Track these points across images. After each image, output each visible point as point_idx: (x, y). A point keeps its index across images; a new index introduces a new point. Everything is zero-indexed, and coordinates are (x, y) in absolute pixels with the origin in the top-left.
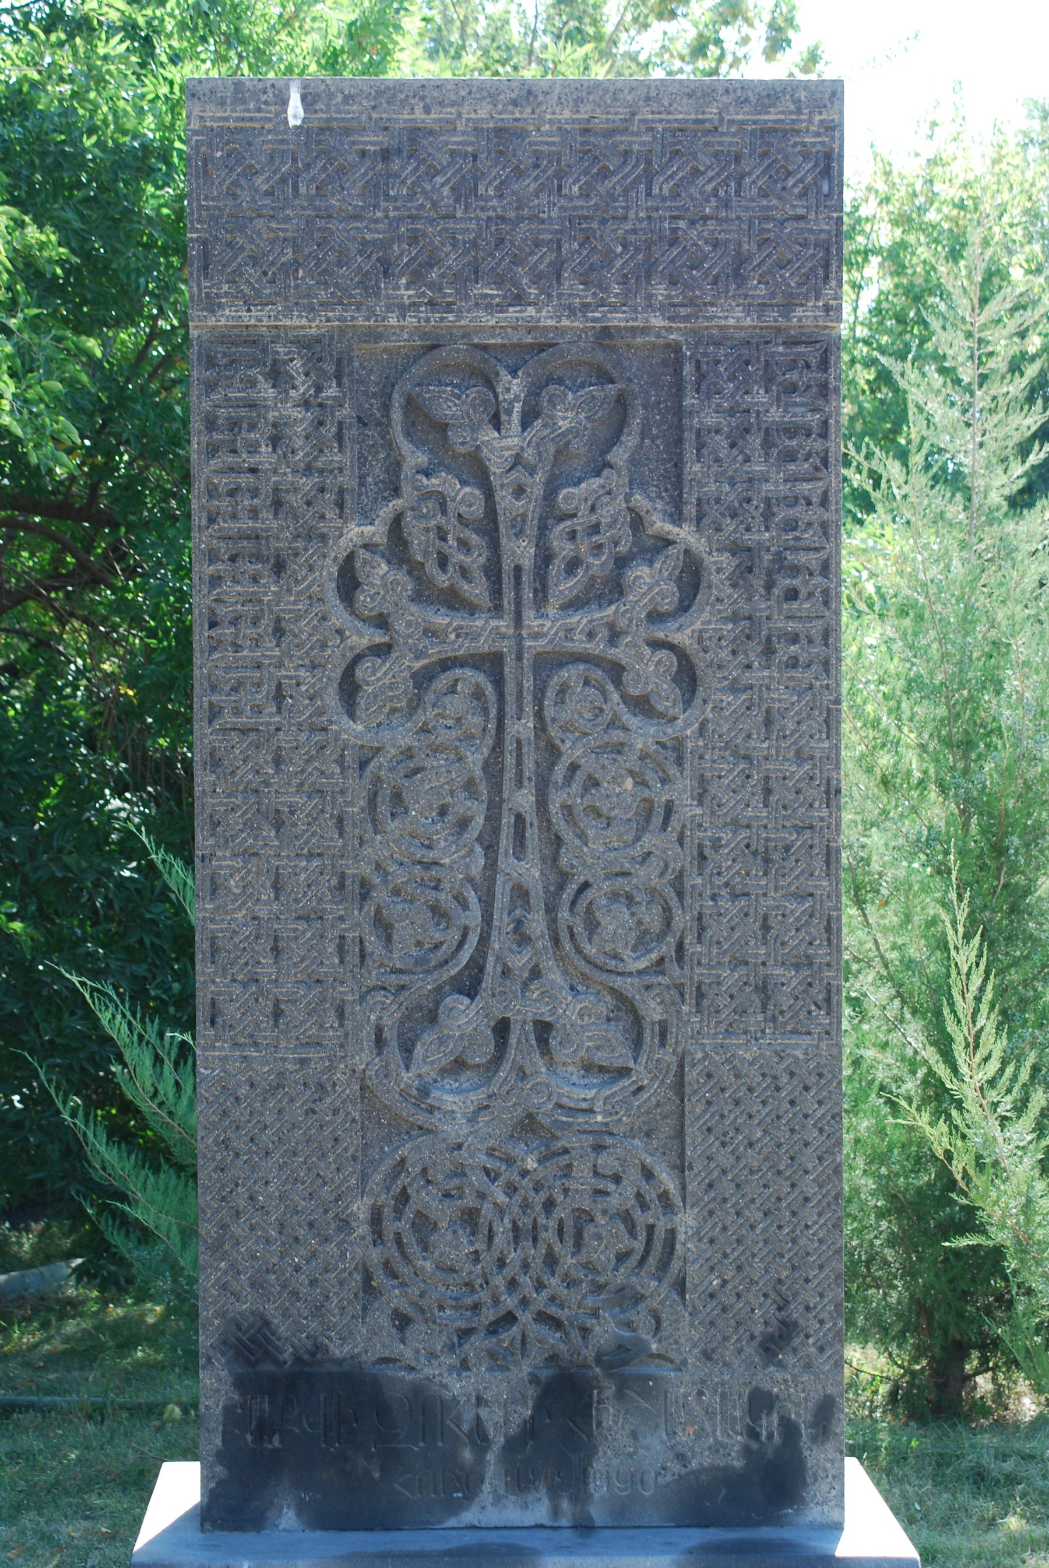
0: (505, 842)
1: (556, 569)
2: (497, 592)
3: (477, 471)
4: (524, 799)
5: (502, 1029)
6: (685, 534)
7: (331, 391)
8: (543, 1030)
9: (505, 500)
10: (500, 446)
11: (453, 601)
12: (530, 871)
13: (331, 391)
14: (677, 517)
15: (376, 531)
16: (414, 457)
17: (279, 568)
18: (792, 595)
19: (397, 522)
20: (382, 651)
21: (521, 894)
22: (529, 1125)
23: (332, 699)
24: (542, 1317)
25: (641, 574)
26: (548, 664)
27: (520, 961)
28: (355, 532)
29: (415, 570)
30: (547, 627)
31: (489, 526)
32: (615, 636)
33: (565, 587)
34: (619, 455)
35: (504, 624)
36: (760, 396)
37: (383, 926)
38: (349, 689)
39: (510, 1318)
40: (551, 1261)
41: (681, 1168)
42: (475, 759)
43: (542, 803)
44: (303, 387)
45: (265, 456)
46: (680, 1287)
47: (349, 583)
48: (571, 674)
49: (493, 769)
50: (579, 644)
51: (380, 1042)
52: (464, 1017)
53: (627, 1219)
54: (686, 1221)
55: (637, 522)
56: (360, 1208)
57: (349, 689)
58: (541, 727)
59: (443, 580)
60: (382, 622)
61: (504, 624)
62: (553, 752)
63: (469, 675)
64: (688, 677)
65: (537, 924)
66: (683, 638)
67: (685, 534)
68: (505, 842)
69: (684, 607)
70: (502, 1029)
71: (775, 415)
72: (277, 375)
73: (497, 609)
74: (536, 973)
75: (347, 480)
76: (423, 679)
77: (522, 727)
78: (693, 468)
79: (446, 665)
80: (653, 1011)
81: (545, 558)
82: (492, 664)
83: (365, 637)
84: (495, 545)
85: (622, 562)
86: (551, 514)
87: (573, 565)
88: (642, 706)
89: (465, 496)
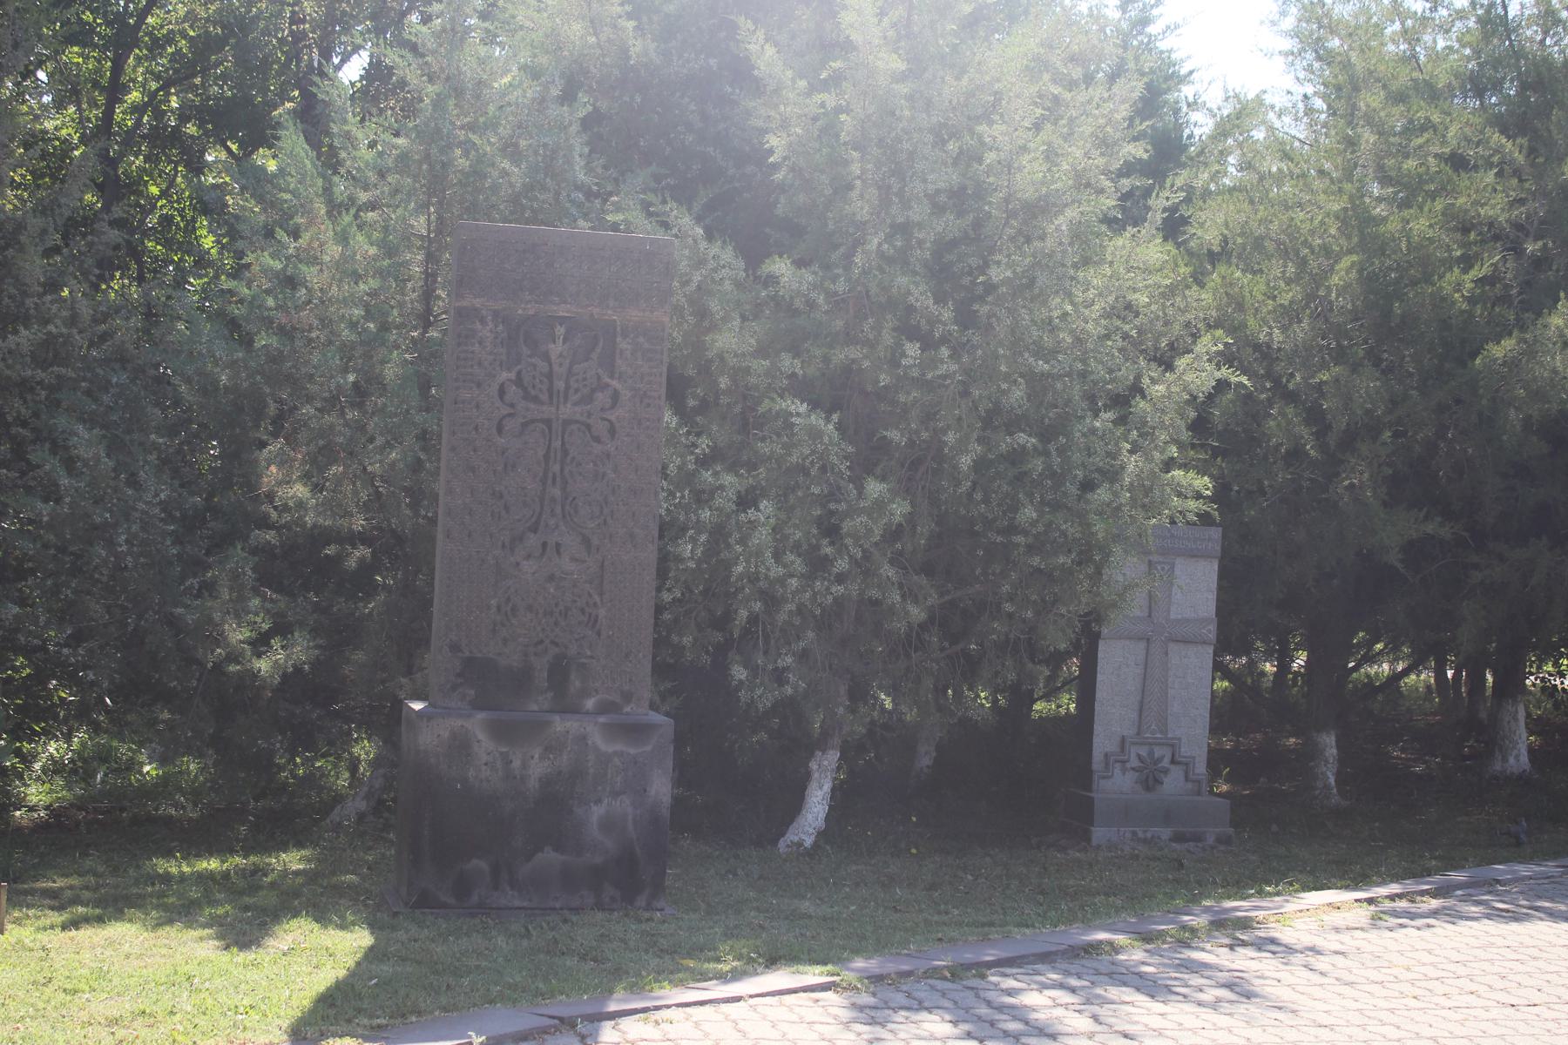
0: (550, 481)
1: (571, 391)
2: (551, 397)
3: (546, 357)
4: (556, 468)
5: (544, 545)
6: (614, 383)
7: (500, 328)
8: (558, 545)
9: (556, 368)
10: (556, 349)
11: (536, 400)
12: (557, 492)
13: (500, 328)
14: (612, 377)
15: (512, 375)
16: (526, 351)
17: (479, 385)
18: (649, 405)
19: (519, 373)
20: (510, 415)
21: (553, 500)
22: (551, 578)
23: (494, 431)
24: (553, 642)
25: (599, 395)
26: (567, 423)
27: (552, 522)
28: (505, 375)
29: (525, 389)
30: (567, 411)
31: (550, 376)
32: (589, 415)
33: (576, 397)
34: (594, 356)
35: (553, 409)
36: (641, 339)
37: (507, 508)
38: (500, 430)
39: (542, 642)
40: (556, 624)
41: (601, 594)
42: (541, 453)
43: (562, 470)
44: (491, 325)
45: (477, 348)
46: (599, 634)
47: (502, 392)
48: (574, 427)
49: (546, 457)
50: (578, 417)
51: (504, 546)
52: (533, 540)
53: (583, 611)
54: (602, 612)
55: (599, 378)
56: (493, 602)
57: (500, 430)
58: (563, 444)
59: (533, 393)
60: (512, 405)
61: (553, 409)
62: (565, 452)
63: (541, 425)
64: (612, 432)
65: (558, 510)
66: (613, 418)
67: (614, 383)
68: (550, 481)
69: (613, 407)
70: (544, 545)
71: (646, 346)
72: (483, 321)
73: (551, 403)
74: (557, 526)
75: (504, 357)
76: (525, 425)
77: (557, 444)
78: (619, 362)
79: (533, 421)
80: (595, 541)
81: (567, 388)
82: (548, 422)
83: (506, 410)
84: (551, 382)
85: (593, 391)
86: (570, 372)
87: (577, 391)
88: (597, 440)
89: (543, 366)
